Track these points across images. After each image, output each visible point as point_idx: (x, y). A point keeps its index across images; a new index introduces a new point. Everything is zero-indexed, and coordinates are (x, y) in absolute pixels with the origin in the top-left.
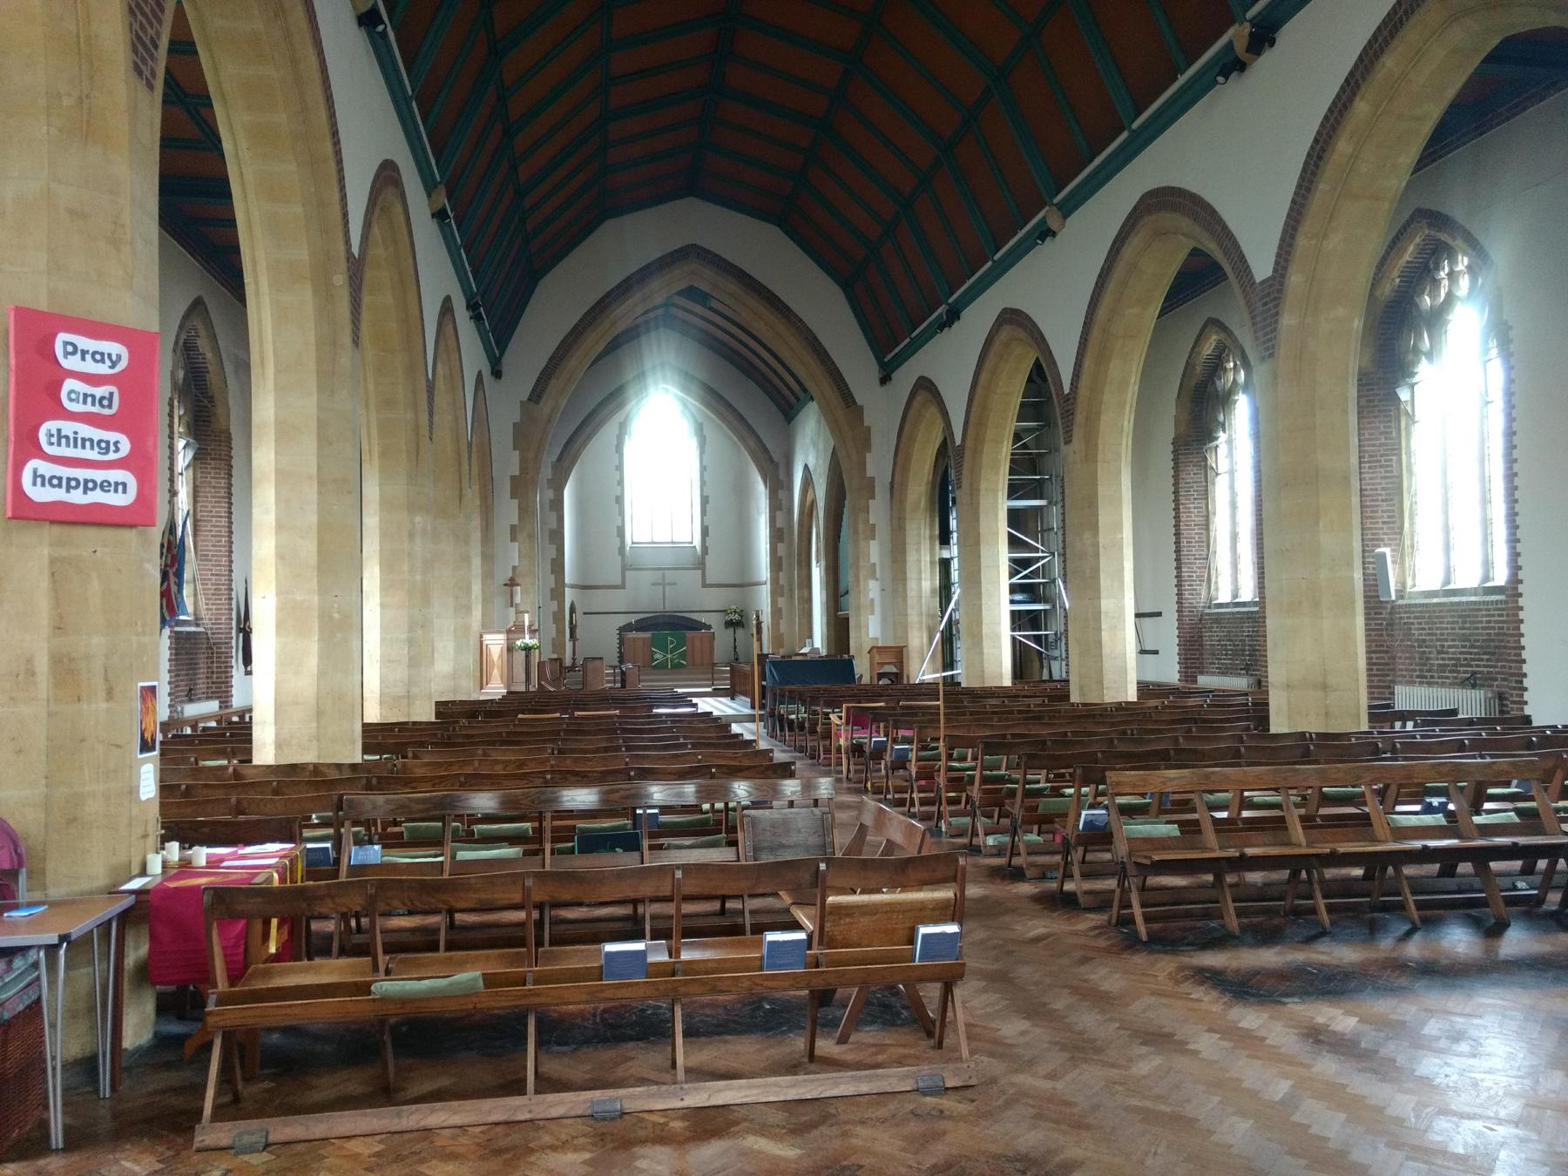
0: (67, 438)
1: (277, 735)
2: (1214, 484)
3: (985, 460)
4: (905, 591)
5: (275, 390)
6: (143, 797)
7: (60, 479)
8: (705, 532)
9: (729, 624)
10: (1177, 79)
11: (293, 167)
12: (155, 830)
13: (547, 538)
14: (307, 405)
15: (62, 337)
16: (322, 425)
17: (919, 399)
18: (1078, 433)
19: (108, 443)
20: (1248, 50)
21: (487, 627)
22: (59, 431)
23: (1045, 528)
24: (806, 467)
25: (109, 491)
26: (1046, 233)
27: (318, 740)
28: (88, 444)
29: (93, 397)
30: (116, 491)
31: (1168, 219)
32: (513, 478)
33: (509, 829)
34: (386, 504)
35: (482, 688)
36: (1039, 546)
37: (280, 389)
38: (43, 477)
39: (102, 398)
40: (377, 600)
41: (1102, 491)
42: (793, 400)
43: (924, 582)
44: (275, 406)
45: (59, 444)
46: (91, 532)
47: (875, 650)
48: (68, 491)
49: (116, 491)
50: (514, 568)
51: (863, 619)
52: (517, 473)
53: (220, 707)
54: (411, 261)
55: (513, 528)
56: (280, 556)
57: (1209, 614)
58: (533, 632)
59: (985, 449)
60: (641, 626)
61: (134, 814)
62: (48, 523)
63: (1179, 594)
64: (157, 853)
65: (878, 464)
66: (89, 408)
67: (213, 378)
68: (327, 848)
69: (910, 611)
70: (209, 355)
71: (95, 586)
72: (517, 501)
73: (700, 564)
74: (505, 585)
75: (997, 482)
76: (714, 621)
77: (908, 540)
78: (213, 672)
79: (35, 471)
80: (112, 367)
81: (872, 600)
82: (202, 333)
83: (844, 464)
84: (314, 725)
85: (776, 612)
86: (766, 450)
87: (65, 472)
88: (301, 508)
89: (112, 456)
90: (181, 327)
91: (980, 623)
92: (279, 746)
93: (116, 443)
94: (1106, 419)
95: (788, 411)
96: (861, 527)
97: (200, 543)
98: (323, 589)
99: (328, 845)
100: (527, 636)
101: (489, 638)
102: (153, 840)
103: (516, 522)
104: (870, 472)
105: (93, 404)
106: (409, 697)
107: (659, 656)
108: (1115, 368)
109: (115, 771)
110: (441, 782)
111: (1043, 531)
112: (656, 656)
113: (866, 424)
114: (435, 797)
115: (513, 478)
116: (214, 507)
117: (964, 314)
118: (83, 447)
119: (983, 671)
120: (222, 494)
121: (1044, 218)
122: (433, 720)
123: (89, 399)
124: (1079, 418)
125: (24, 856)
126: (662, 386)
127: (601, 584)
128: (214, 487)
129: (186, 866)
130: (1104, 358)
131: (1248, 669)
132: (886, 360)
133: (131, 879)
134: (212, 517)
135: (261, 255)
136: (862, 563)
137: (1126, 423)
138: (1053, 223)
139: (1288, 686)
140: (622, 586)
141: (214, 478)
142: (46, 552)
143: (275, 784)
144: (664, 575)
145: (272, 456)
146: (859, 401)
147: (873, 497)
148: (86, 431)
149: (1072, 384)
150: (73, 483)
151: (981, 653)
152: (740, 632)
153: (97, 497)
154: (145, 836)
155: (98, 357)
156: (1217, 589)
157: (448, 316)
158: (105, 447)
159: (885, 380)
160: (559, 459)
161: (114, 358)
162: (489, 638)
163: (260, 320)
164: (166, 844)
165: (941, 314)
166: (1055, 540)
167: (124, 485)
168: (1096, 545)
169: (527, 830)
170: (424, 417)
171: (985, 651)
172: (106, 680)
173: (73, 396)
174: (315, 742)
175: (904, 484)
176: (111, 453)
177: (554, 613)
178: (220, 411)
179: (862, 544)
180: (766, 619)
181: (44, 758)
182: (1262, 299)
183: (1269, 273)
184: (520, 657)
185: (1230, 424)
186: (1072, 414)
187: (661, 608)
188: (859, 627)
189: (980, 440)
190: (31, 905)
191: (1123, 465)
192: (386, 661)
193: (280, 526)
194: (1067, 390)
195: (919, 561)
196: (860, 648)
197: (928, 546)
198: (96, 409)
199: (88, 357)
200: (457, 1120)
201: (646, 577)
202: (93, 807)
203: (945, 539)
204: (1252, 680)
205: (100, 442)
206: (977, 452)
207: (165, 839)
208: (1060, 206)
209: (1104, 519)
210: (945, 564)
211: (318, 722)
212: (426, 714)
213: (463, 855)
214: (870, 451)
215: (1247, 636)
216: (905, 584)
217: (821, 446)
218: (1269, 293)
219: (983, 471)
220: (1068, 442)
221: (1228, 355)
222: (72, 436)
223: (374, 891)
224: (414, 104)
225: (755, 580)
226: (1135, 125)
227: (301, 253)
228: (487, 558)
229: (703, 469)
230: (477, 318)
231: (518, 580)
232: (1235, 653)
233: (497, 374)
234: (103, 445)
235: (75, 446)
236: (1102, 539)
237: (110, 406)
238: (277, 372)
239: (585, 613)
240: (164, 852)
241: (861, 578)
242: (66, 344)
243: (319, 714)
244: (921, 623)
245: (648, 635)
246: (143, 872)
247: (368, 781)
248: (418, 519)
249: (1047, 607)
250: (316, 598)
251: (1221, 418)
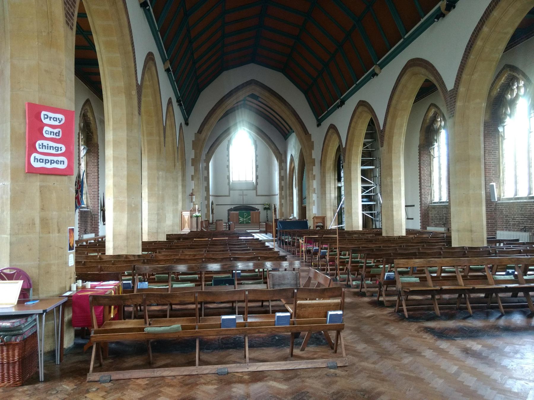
0: (45, 146)
1: (114, 245)
2: (433, 161)
3: (353, 152)
4: (325, 197)
5: (113, 130)
6: (70, 265)
7: (43, 160)
8: (257, 177)
9: (265, 209)
10: (421, 20)
11: (119, 55)
12: (74, 276)
13: (204, 180)
14: (123, 134)
15: (43, 113)
16: (128, 141)
17: (330, 131)
18: (385, 144)
19: (58, 148)
20: (446, 10)
21: (184, 209)
22: (42, 144)
23: (374, 176)
24: (291, 155)
25: (58, 164)
26: (374, 74)
27: (127, 247)
28: (52, 148)
29: (53, 132)
30: (61, 164)
31: (416, 69)
32: (192, 159)
33: (191, 277)
34: (150, 168)
35: (182, 230)
36: (372, 182)
37: (114, 130)
38: (37, 159)
39: (56, 133)
40: (147, 200)
41: (394, 163)
42: (287, 132)
43: (332, 194)
44: (113, 135)
45: (42, 148)
46: (53, 177)
47: (315, 218)
48: (45, 164)
49: (61, 164)
50: (193, 189)
51: (311, 207)
52: (194, 158)
53: (95, 236)
54: (158, 86)
55: (192, 176)
56: (115, 186)
57: (431, 206)
58: (199, 211)
59: (353, 149)
60: (235, 209)
61: (67, 271)
62: (39, 174)
63: (421, 199)
64: (75, 283)
65: (316, 154)
66: (52, 136)
67: (92, 126)
68: (130, 283)
69: (327, 204)
70: (91, 118)
71: (54, 195)
72: (194, 167)
73: (255, 188)
74: (190, 195)
75: (357, 160)
76: (260, 208)
77: (326, 180)
78: (93, 224)
79: (35, 157)
80: (60, 122)
81: (314, 201)
82: (89, 111)
83: (305, 154)
84: (126, 242)
85: (281, 205)
86: (278, 149)
87: (45, 157)
88: (121, 169)
89: (59, 152)
90: (82, 109)
91: (351, 209)
92: (114, 249)
93: (61, 148)
94: (395, 138)
95: (285, 135)
96: (310, 176)
97: (88, 181)
98: (129, 196)
99: (130, 282)
100: (197, 212)
101: (184, 213)
102: (73, 279)
103: (193, 174)
104: (313, 157)
105: (53, 135)
106: (157, 233)
107: (241, 219)
108: (398, 121)
109: (61, 257)
110: (168, 261)
111: (373, 177)
112: (240, 219)
113: (312, 140)
114: (166, 266)
115: (192, 159)
116: (93, 169)
117: (346, 103)
118: (50, 149)
119: (352, 225)
120: (96, 165)
121: (374, 69)
122: (166, 240)
123: (52, 133)
124: (386, 138)
125: (32, 284)
126: (243, 128)
127: (223, 195)
128: (93, 162)
129: (84, 288)
130: (394, 117)
131: (444, 225)
132: (319, 118)
133: (66, 292)
134: (93, 172)
135: (108, 84)
136: (310, 188)
137: (402, 140)
138: (377, 71)
139: (458, 231)
140: (229, 196)
141: (93, 159)
142: (38, 184)
143: (113, 261)
144: (243, 192)
145: (112, 152)
146: (310, 133)
147: (314, 165)
148: (51, 144)
149: (383, 126)
150: (47, 161)
151: (352, 219)
152: (269, 211)
153: (55, 166)
154: (71, 278)
155: (55, 119)
156: (434, 197)
157: (170, 104)
158: (57, 149)
159: (319, 125)
160: (208, 153)
161: (60, 120)
162: (184, 213)
163: (108, 106)
164: (78, 281)
165: (338, 103)
166: (378, 180)
167: (63, 161)
168: (392, 182)
169: (196, 277)
170: (162, 139)
171: (353, 218)
172: (58, 226)
173: (47, 132)
174: (126, 248)
175: (325, 161)
176: (59, 151)
177: (206, 204)
178: (95, 137)
179: (311, 181)
180: (278, 207)
181: (38, 252)
182: (450, 96)
183: (453, 87)
184: (194, 219)
185: (439, 140)
186: (383, 137)
188: (309, 210)
189: (351, 146)
190: (34, 300)
191: (401, 154)
192: (150, 221)
193: (114, 175)
194: (381, 128)
195: (330, 187)
196: (310, 217)
197: (333, 182)
198: (54, 137)
199: (52, 119)
200: (173, 374)
201: (237, 193)
202: (54, 268)
203: (339, 180)
204: (446, 229)
205: (55, 147)
206: (350, 150)
207: (77, 279)
208: (379, 65)
209: (394, 173)
210: (339, 188)
211: (127, 241)
212: (163, 238)
213: (175, 286)
214: (313, 150)
215: (444, 213)
216: (325, 195)
217: (297, 148)
218: (452, 95)
219: (352, 156)
220: (382, 146)
221: (438, 116)
222: (46, 145)
223: (145, 297)
224: (159, 33)
225: (274, 194)
226: (406, 37)
227: (121, 84)
228: (184, 186)
229: (256, 156)
230: (180, 105)
231: (194, 194)
232: (440, 220)
233: (187, 124)
234: (57, 148)
235: (48, 149)
236: (394, 180)
237: (59, 135)
238: (113, 123)
240: (77, 283)
241: (310, 193)
242: (45, 115)
243: (128, 238)
244: (331, 208)
245: (238, 212)
246: (70, 290)
247: (143, 261)
248: (160, 173)
249: (375, 203)
250: (126, 199)
251: (435, 138)
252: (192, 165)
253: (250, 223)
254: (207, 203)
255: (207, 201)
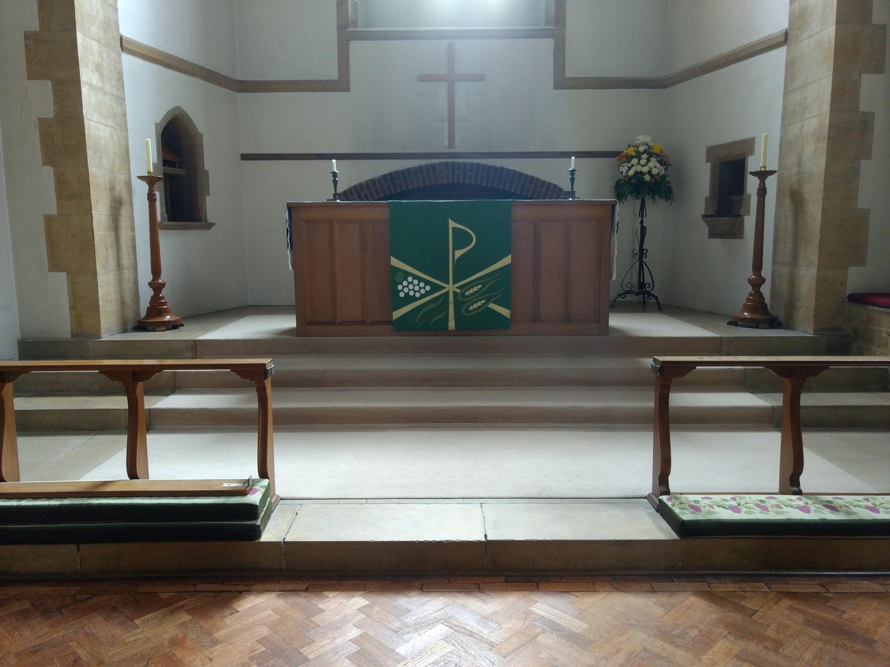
112: (405, 288)
140: (341, 84)
152: (656, 211)
177: (44, 123)
187: (442, 146)
239: (245, 157)
253: (496, 324)
254: (49, 112)
255: (45, 88)
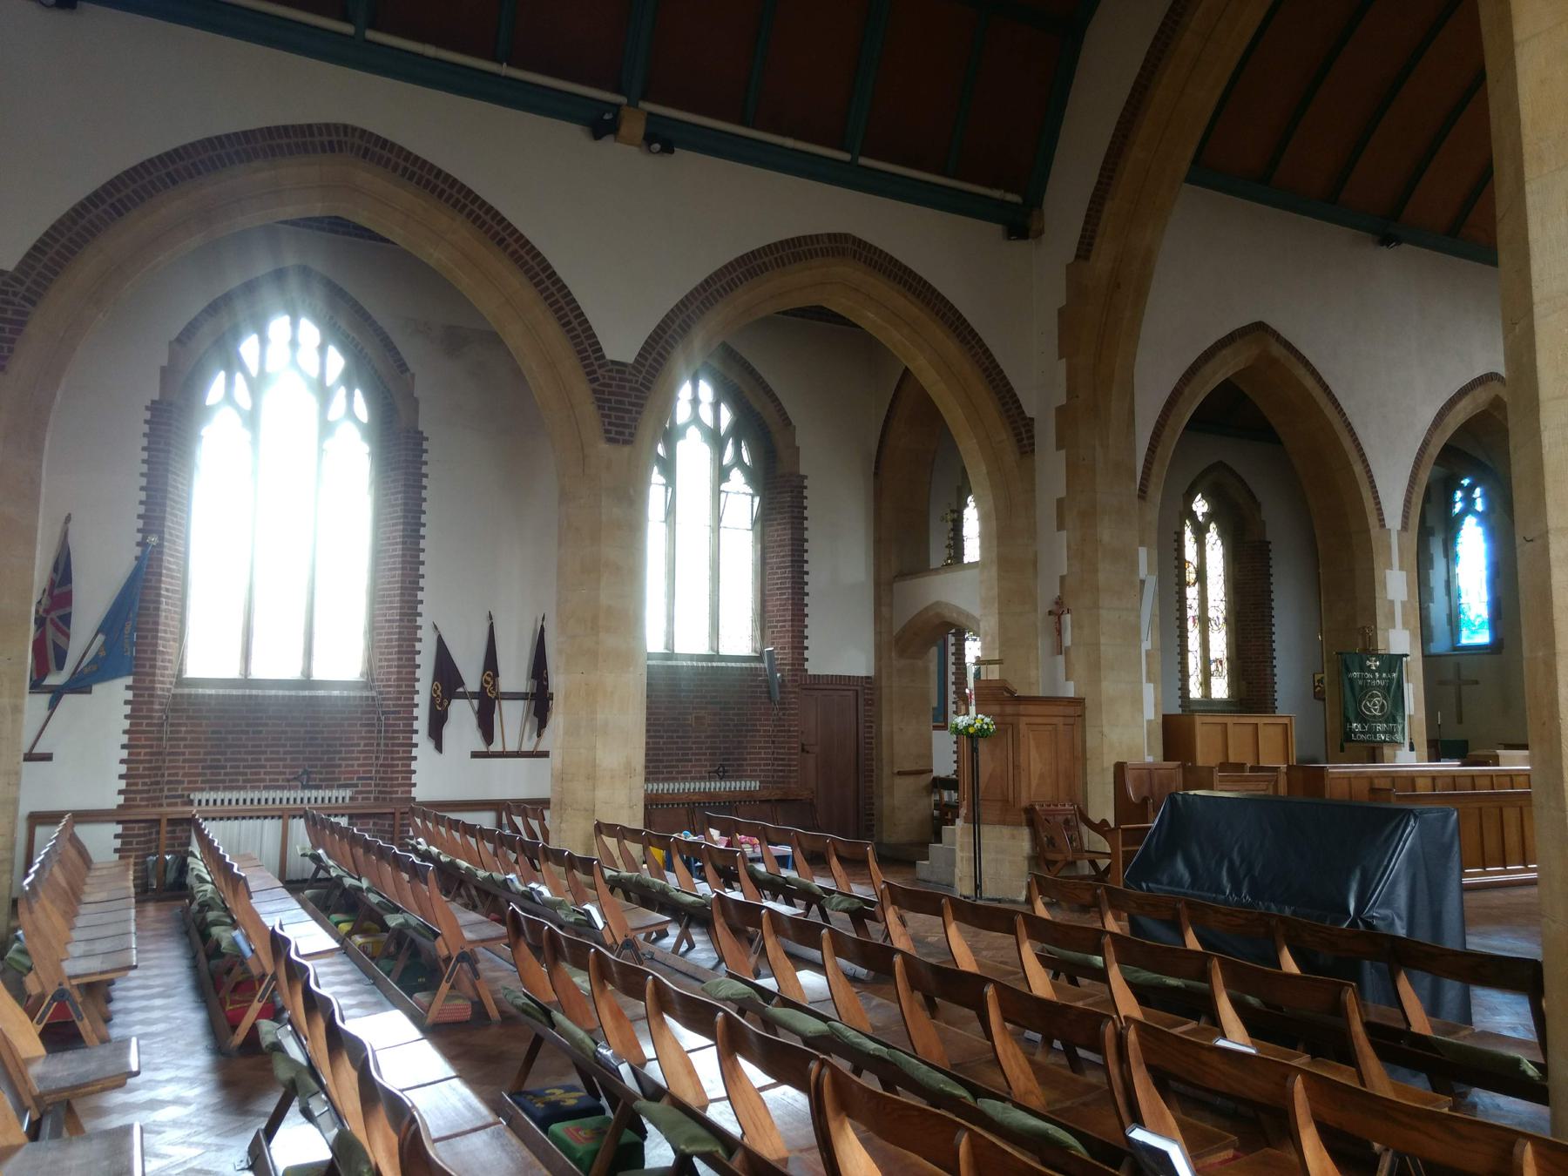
50: (1063, 578)
55: (1060, 502)
74: (1050, 613)
103: (1062, 493)
252: (1059, 447)
